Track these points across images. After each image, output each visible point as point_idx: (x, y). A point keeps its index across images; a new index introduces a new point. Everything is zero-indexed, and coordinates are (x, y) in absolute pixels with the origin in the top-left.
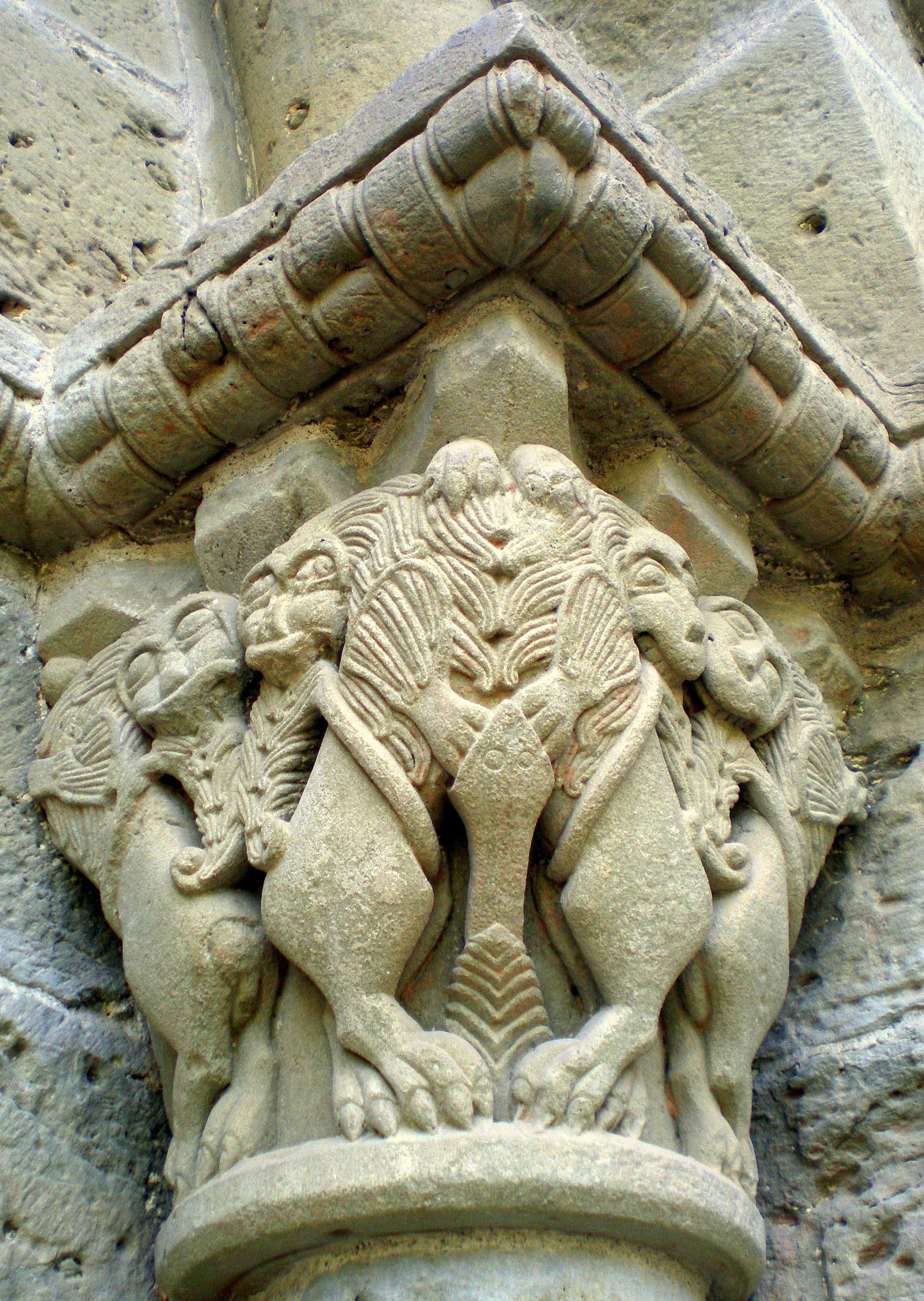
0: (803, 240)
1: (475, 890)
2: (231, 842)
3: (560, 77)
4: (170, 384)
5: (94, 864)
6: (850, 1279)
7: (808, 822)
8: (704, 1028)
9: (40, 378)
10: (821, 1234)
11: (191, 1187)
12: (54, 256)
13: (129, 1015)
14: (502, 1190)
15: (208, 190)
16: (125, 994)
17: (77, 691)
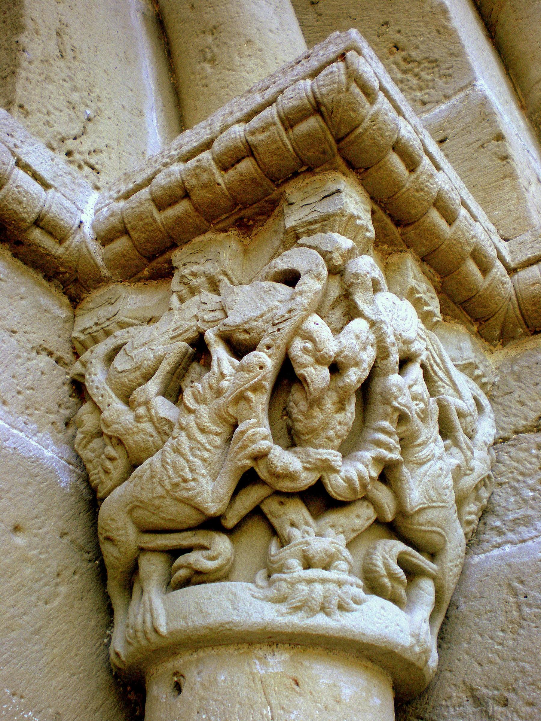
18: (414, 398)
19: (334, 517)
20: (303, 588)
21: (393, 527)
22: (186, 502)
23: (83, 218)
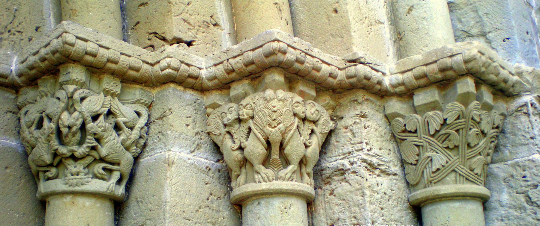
0: (334, 15)
1: (272, 151)
2: (239, 144)
3: (281, 41)
4: (225, 74)
5: (218, 143)
6: (327, 198)
7: (322, 134)
8: (305, 165)
9: (203, 66)
10: (324, 191)
11: (236, 188)
12: (198, 28)
13: (223, 162)
17: (213, 116)
18: (99, 127)
19: (79, 162)
20: (71, 181)
21: (102, 160)
22: (43, 161)
23: (12, 68)
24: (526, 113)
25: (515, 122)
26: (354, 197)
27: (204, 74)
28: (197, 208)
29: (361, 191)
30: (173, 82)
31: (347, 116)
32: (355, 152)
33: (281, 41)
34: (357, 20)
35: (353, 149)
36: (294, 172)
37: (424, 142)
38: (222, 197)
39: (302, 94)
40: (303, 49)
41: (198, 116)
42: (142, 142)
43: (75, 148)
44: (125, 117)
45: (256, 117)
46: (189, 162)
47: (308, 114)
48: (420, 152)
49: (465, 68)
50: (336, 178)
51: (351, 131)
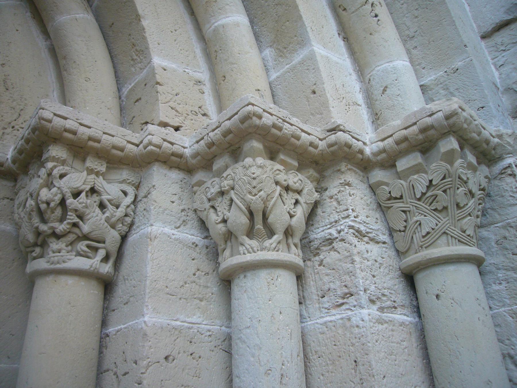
0: (312, 96)
2: (222, 216)
3: (256, 106)
4: (206, 148)
5: (204, 219)
6: (317, 269)
7: (307, 204)
8: (292, 236)
9: (186, 145)
13: (212, 239)
14: (261, 260)
15: (210, 91)
16: (210, 236)
17: (198, 193)
18: (80, 203)
20: (52, 258)
24: (510, 175)
25: (499, 184)
26: (344, 265)
27: (188, 152)
28: (181, 283)
29: (350, 258)
30: (157, 160)
31: (332, 186)
32: (341, 219)
33: (256, 106)
34: (334, 97)
35: (339, 217)
36: (279, 242)
37: (411, 206)
38: (210, 272)
39: (283, 163)
40: (280, 116)
41: (185, 194)
42: (128, 220)
43: (56, 225)
44: (109, 195)
45: (237, 187)
46: (173, 237)
47: (291, 183)
48: (407, 218)
49: (446, 125)
50: (324, 248)
51: (336, 199)
